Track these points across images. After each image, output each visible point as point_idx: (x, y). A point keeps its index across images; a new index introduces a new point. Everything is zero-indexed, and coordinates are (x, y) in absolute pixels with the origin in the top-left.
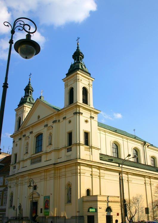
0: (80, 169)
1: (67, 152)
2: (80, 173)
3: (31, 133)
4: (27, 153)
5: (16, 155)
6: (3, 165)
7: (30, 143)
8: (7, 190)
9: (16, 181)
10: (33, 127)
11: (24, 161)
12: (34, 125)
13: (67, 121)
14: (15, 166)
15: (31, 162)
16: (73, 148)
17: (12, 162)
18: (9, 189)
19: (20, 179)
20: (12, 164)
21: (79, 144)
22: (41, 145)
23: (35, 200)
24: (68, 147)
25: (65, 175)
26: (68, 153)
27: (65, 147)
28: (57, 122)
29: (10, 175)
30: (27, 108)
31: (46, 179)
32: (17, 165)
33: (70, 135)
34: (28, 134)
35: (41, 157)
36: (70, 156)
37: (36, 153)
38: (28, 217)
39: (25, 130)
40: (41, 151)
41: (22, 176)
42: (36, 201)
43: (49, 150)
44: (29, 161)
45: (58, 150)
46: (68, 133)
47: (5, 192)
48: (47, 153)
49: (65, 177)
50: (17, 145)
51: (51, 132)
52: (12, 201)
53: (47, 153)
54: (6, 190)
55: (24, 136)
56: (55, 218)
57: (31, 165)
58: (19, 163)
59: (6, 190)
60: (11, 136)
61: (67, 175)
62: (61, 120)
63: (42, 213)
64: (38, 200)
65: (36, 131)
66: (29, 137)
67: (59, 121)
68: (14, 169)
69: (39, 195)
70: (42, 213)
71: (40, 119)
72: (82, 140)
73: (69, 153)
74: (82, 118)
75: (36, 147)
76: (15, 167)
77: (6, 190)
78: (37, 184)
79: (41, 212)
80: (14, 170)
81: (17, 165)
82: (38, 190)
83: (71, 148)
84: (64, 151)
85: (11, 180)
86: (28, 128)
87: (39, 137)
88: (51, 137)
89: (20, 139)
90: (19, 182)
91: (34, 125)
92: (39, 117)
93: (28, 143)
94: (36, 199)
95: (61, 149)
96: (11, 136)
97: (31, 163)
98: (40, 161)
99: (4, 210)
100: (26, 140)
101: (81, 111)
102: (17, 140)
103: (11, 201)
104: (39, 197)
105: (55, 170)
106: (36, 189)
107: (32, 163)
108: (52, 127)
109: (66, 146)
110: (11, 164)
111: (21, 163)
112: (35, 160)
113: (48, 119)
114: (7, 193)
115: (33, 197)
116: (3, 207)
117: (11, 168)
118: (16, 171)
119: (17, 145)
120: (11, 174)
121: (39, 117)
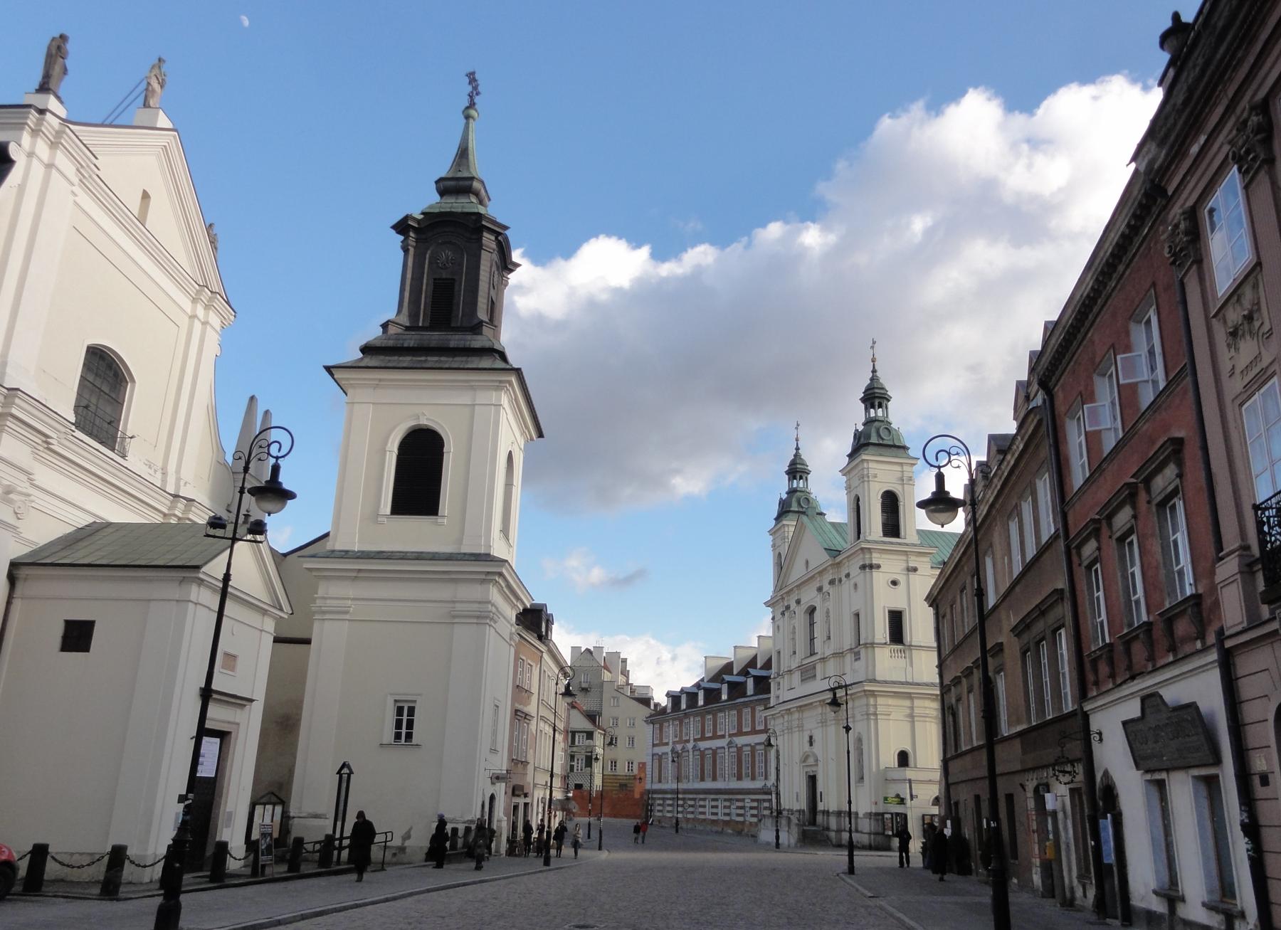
0: (875, 706)
2: (875, 714)
4: (795, 653)
7: (796, 625)
10: (798, 587)
12: (801, 586)
13: (852, 582)
20: (775, 678)
21: (872, 645)
27: (851, 649)
31: (826, 722)
33: (857, 615)
34: (793, 605)
35: (815, 668)
38: (804, 811)
43: (828, 653)
44: (797, 676)
45: (839, 655)
53: (823, 659)
55: (788, 607)
60: (768, 604)
62: (844, 579)
67: (840, 581)
69: (817, 760)
72: (882, 630)
73: (857, 663)
74: (879, 579)
84: (849, 658)
90: (786, 724)
91: (801, 586)
92: (807, 562)
93: (794, 627)
94: (814, 769)
96: (768, 604)
97: (802, 681)
100: (791, 618)
101: (874, 562)
102: (779, 616)
104: (817, 765)
109: (853, 647)
112: (808, 673)
113: (821, 573)
120: (772, 702)
121: (807, 562)
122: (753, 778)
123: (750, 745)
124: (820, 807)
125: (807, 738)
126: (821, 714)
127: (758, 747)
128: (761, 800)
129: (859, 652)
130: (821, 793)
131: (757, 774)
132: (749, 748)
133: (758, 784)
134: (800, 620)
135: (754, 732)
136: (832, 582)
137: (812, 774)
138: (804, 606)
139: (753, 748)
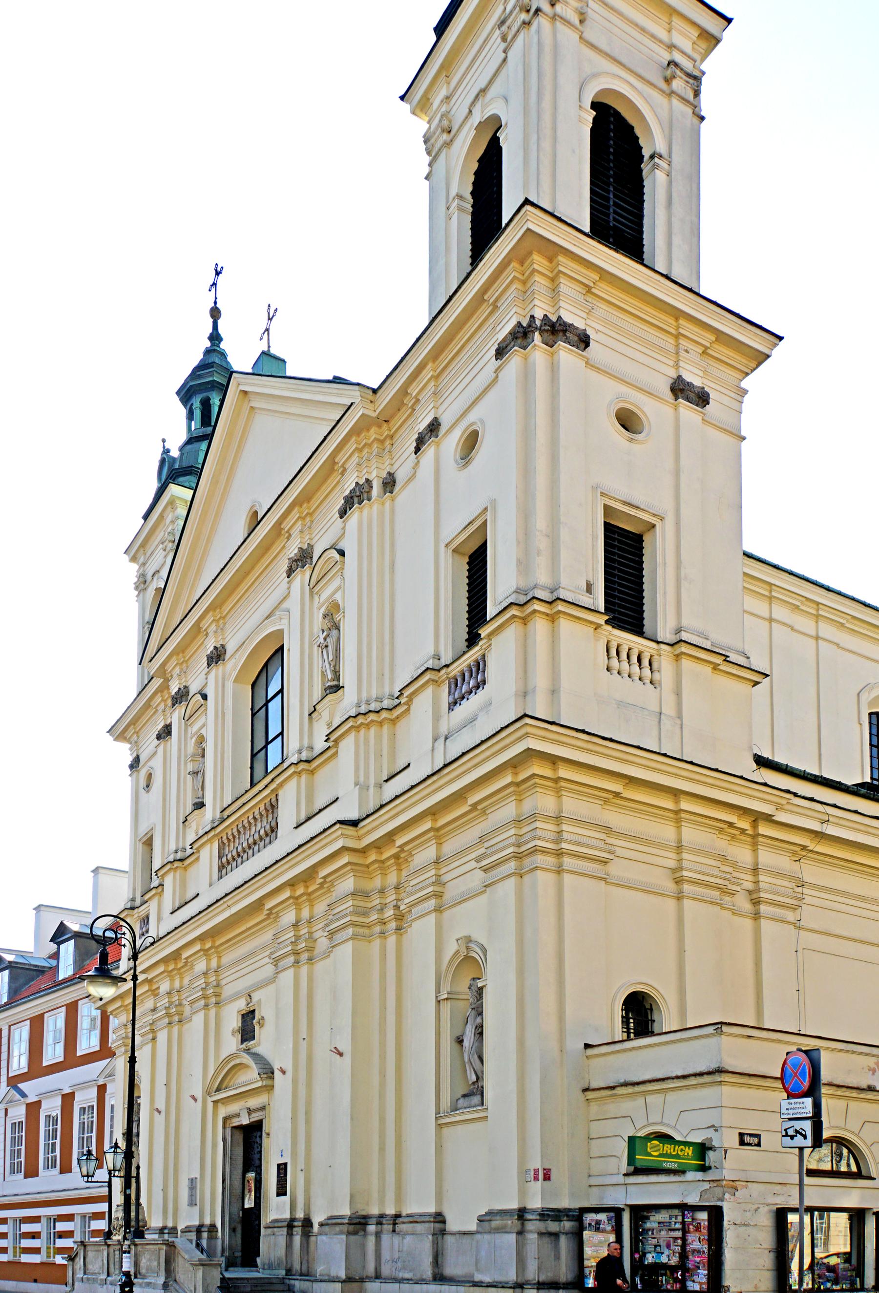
15: (220, 857)
23: (250, 1111)
25: (438, 895)
31: (310, 949)
38: (212, 1228)
42: (255, 1117)
49: (438, 910)
56: (372, 1228)
61: (452, 891)
63: (285, 1194)
64: (263, 1108)
69: (268, 1072)
70: (285, 1194)
79: (281, 1191)
82: (264, 1042)
94: (254, 1102)
105: (361, 870)
106: (253, 1038)
125: (233, 1022)
126: (296, 925)
130: (282, 1169)
137: (245, 1121)
138: (232, 665)
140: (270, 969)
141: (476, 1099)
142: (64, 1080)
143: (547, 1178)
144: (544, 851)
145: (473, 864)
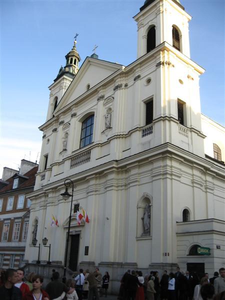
1: (143, 136)
3: (74, 115)
5: (46, 157)
6: (28, 178)
8: (29, 217)
9: (43, 199)
11: (59, 164)
14: (44, 176)
16: (158, 127)
17: (39, 170)
18: (32, 214)
19: (50, 195)
22: (91, 134)
23: (76, 231)
24: (144, 128)
26: (144, 137)
28: (123, 87)
29: (35, 189)
30: (67, 81)
32: (47, 174)
36: (149, 142)
37: (80, 148)
38: (61, 262)
39: (64, 113)
40: (90, 143)
41: (54, 190)
42: (78, 233)
46: (144, 102)
47: (26, 219)
48: (102, 145)
50: (49, 140)
51: (111, 107)
52: (36, 234)
53: (102, 145)
54: (28, 215)
57: (71, 168)
58: (51, 169)
59: (28, 215)
64: (81, 231)
65: (82, 111)
66: (70, 124)
68: (42, 180)
71: (90, 88)
75: (81, 140)
76: (43, 177)
77: (27, 216)
78: (79, 202)
80: (43, 181)
81: (47, 174)
83: (151, 128)
85: (37, 197)
86: (69, 109)
87: (88, 119)
88: (109, 115)
89: (55, 130)
92: (89, 86)
95: (130, 133)
96: (42, 129)
97: (71, 166)
98: (89, 159)
99: (23, 249)
103: (35, 233)
107: (72, 166)
108: (113, 98)
110: (38, 172)
111: (55, 168)
114: (28, 221)
115: (69, 225)
116: (22, 244)
117: (38, 178)
118: (45, 182)
119: (49, 140)
120: (36, 187)
121: (89, 86)
122: (10, 240)
123: (10, 219)
124: (82, 258)
127: (16, 221)
128: (13, 255)
129: (152, 127)
130: (87, 248)
131: (13, 237)
132: (9, 221)
133: (13, 244)
134: (76, 127)
135: (15, 210)
136: (117, 88)
139: (12, 221)
140: (84, 195)
141: (148, 234)
142: (12, 216)
143: (168, 255)
144: (169, 174)
145: (149, 174)
